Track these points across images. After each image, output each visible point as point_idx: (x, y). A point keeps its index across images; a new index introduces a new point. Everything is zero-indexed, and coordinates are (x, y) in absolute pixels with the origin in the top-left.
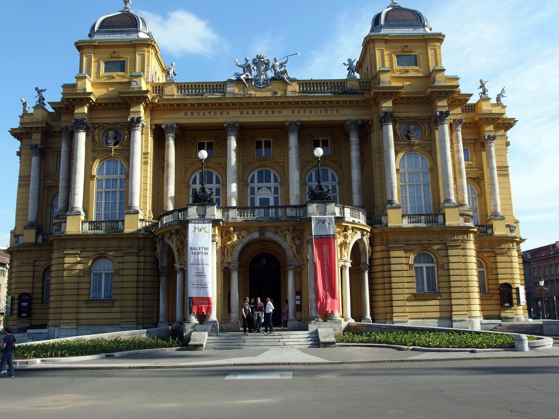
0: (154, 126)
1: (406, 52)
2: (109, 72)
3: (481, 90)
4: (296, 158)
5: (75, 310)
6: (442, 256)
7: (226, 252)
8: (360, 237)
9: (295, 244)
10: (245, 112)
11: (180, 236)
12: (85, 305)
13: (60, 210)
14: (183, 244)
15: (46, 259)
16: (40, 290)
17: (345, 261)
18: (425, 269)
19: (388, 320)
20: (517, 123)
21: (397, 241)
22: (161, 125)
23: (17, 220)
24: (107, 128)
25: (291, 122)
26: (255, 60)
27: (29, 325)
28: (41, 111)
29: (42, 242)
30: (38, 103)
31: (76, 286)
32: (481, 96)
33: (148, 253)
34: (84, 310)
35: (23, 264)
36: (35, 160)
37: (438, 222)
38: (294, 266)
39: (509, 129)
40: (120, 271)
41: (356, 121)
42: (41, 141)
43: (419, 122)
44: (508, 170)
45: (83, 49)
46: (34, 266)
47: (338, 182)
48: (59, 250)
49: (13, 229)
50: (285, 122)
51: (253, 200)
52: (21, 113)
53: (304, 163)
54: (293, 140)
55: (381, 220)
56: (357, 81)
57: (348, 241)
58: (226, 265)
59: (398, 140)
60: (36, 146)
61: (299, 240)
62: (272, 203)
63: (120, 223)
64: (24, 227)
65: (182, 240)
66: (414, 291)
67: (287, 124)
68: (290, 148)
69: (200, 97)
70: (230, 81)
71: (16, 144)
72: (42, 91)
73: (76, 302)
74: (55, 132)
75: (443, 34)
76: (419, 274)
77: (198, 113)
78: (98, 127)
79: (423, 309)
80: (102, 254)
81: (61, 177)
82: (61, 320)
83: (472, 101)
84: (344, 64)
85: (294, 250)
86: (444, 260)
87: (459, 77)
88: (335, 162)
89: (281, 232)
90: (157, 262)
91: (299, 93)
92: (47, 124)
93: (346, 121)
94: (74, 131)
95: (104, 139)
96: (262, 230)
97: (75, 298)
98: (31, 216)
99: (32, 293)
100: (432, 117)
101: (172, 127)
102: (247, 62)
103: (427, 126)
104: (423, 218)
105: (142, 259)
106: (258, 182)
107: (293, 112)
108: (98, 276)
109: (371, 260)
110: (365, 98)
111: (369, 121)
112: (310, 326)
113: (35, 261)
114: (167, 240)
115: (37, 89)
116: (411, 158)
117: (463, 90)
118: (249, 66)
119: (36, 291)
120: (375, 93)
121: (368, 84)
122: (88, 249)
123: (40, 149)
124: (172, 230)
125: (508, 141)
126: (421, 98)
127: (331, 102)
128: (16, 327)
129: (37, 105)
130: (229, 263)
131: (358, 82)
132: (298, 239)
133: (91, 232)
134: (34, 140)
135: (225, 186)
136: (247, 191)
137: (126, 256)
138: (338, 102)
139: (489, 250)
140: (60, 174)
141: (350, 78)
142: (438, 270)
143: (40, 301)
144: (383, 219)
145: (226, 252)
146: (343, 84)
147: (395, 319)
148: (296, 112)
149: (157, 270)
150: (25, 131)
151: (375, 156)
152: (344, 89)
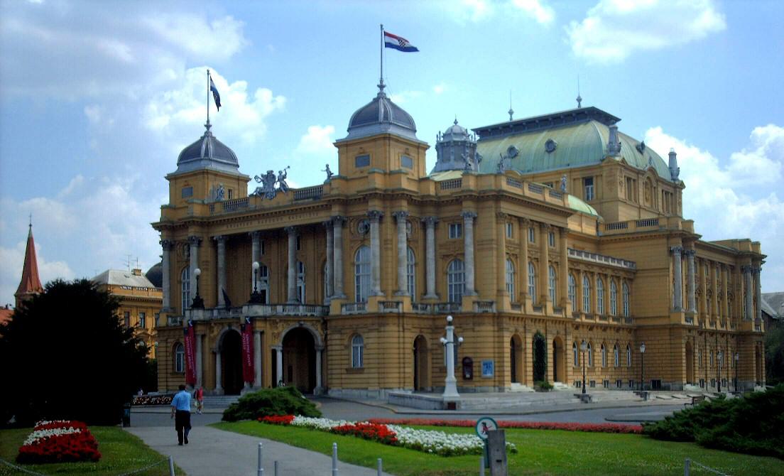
10: (261, 221)
22: (213, 237)
34: (170, 380)
41: (328, 222)
79: (354, 381)
96: (230, 325)
104: (356, 306)
148: (291, 218)
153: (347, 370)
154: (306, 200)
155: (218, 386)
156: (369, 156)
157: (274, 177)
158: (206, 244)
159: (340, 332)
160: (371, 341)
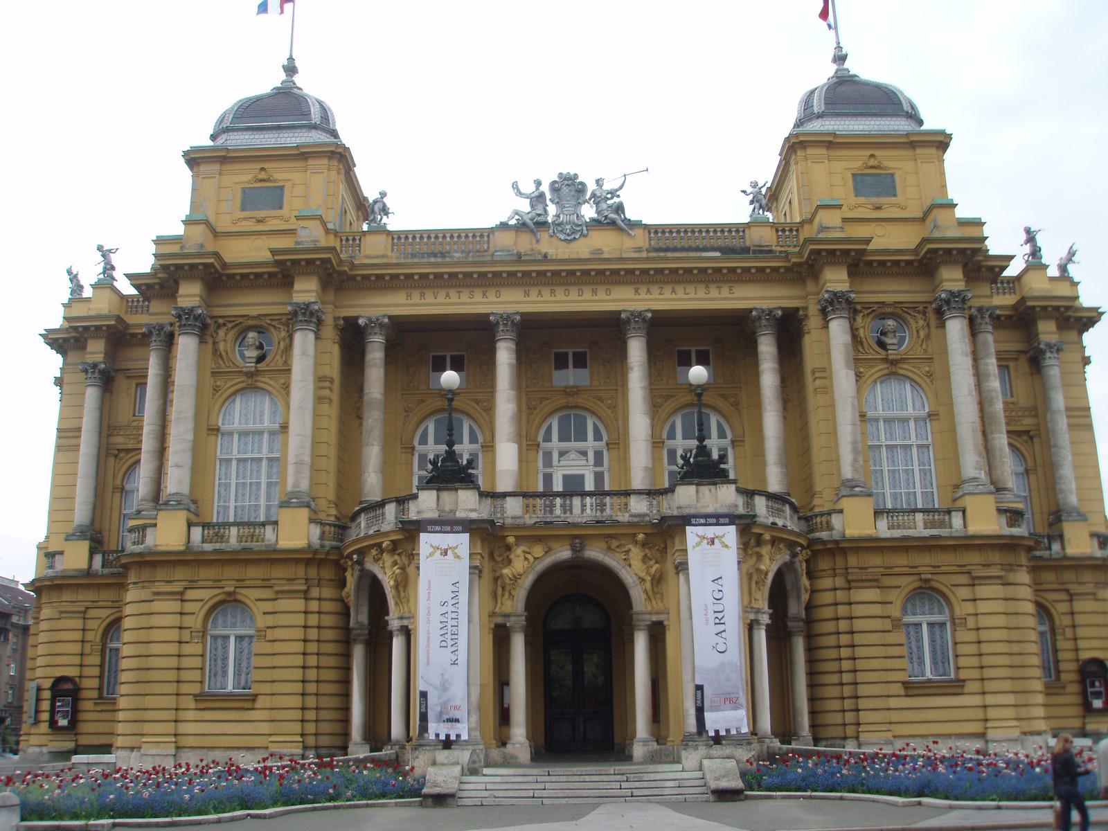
0: (342, 322)
1: (872, 167)
2: (250, 210)
3: (1027, 249)
4: (644, 388)
5: (170, 715)
6: (963, 600)
7: (500, 590)
8: (787, 558)
9: (648, 573)
11: (399, 554)
12: (193, 705)
13: (142, 500)
14: (406, 573)
15: (110, 603)
16: (96, 671)
17: (758, 611)
18: (925, 627)
19: (848, 741)
20: (1103, 317)
21: (866, 568)
22: (357, 318)
23: (52, 522)
24: (243, 325)
25: (632, 313)
26: (554, 182)
27: (70, 745)
28: (107, 292)
29: (103, 566)
30: (102, 276)
31: (173, 662)
32: (1027, 261)
33: (328, 592)
34: (191, 715)
35: (63, 615)
36: (91, 395)
37: (951, 528)
38: (648, 623)
39: (1087, 330)
40: (268, 630)
41: (771, 311)
42: (105, 354)
43: (904, 314)
44: (1089, 416)
45: (198, 164)
46: (84, 619)
47: (733, 442)
48: (140, 585)
49: (42, 539)
50: (619, 312)
51: (548, 479)
52: (66, 296)
53: (659, 401)
54: (636, 350)
55: (828, 523)
56: (772, 227)
57: (763, 567)
58: (499, 620)
59: (861, 350)
60: (95, 366)
61: (657, 566)
62: (589, 486)
63: (269, 529)
64: (65, 535)
65: (404, 564)
66: (903, 677)
67: (623, 316)
68: (632, 369)
69: (440, 260)
70: (504, 226)
71: (55, 361)
72: (110, 251)
73: (175, 697)
74: (134, 335)
75: (948, 132)
76: (913, 639)
77: (434, 293)
78: (225, 325)
80: (229, 594)
81: (146, 430)
82: (143, 735)
83: (1013, 270)
84: (744, 192)
85: (648, 585)
86: (969, 608)
87: (983, 221)
88: (724, 397)
89: (618, 547)
90: (345, 613)
91: (648, 251)
92: (119, 319)
93: (750, 310)
94: (177, 333)
95: (237, 349)
97: (172, 688)
98: (81, 513)
99: (80, 677)
100: (931, 303)
101: (381, 325)
102: (537, 189)
103: (921, 323)
104: (919, 517)
105: (314, 606)
106: (561, 439)
107: (636, 291)
108: (219, 641)
109: (809, 607)
110: (790, 261)
111: (797, 309)
112: (684, 754)
113: (87, 608)
114: (371, 566)
115: (100, 248)
116: (891, 385)
117: (995, 247)
118: (542, 195)
119: (88, 671)
120: (813, 252)
121: (795, 233)
122: (200, 584)
123: (102, 372)
124: (382, 543)
125: (1086, 355)
126: (909, 263)
127: (718, 270)
128: (45, 750)
129: (99, 280)
130: (507, 616)
131: (774, 230)
132: (656, 563)
133: (208, 547)
134: (91, 353)
135: (489, 447)
136: (536, 461)
137: (282, 598)
138: (732, 270)
139: (1056, 586)
140: (145, 424)
141: (755, 223)
142: (954, 631)
143: (95, 694)
144: (836, 520)
145: (500, 590)
146: (741, 234)
147: (863, 737)
149: (346, 629)
150: (72, 334)
151: (810, 384)
152: (744, 242)
153: (906, 685)
155: (519, 731)
156: (892, 175)
157: (581, 189)
158: (329, 332)
159: (874, 583)
160: (983, 607)
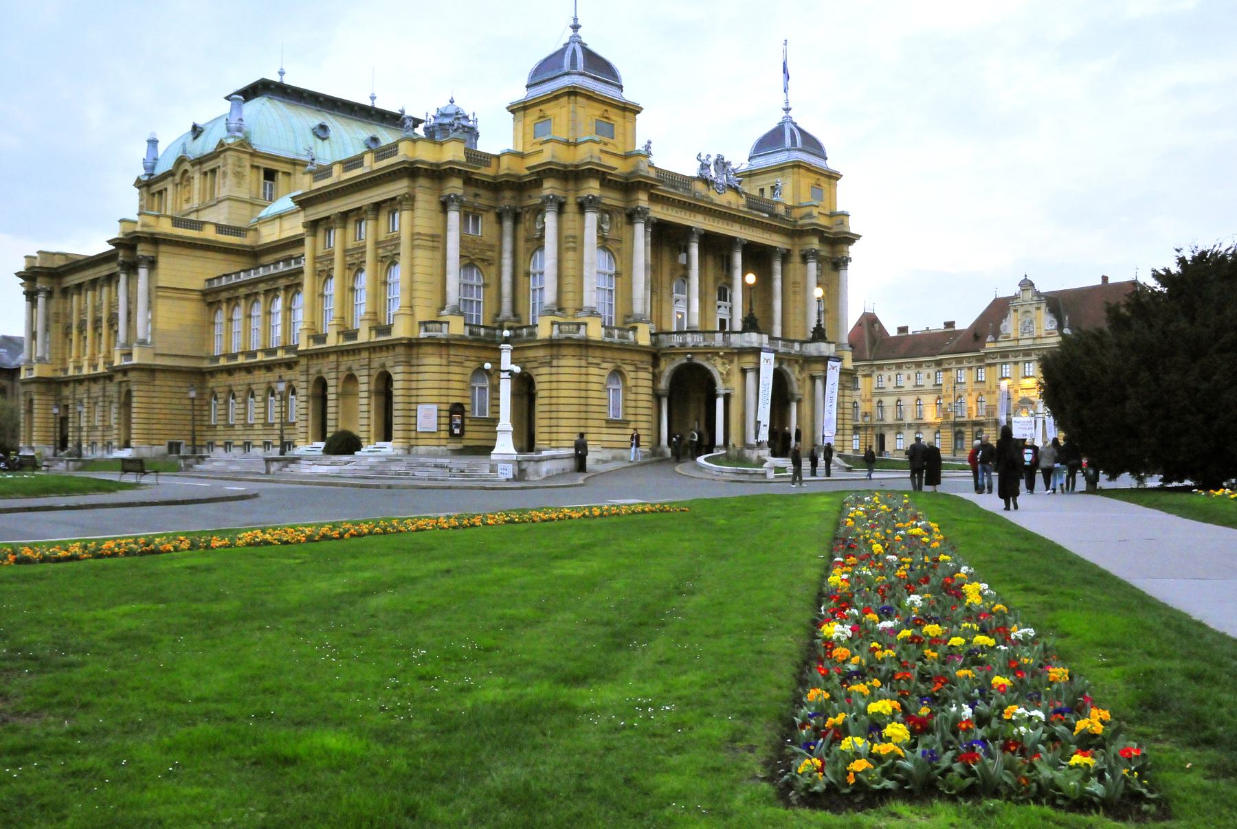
34: (604, 430)
154: (756, 212)
